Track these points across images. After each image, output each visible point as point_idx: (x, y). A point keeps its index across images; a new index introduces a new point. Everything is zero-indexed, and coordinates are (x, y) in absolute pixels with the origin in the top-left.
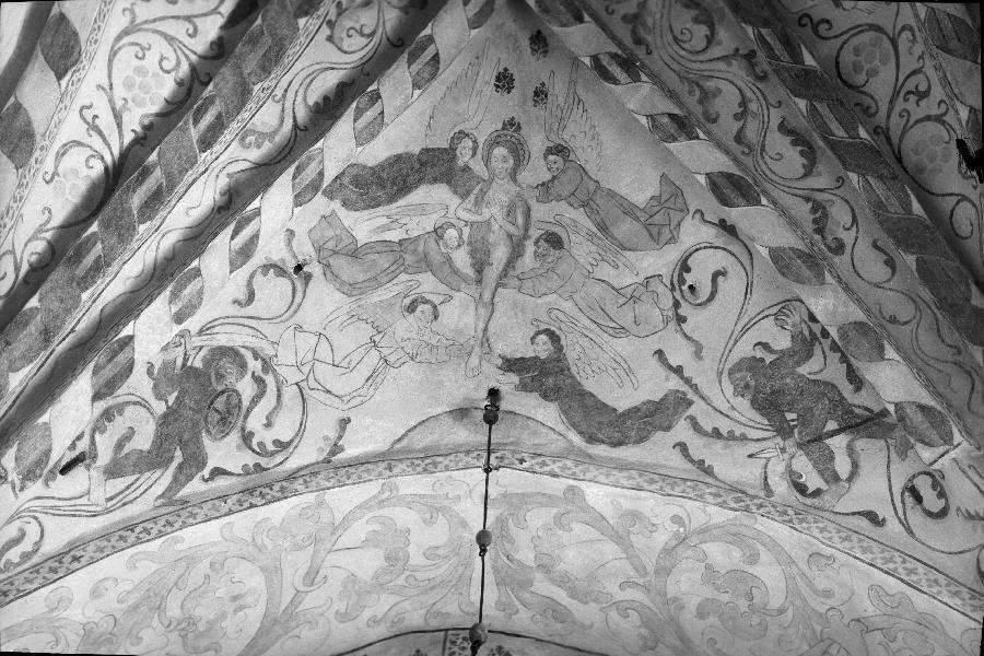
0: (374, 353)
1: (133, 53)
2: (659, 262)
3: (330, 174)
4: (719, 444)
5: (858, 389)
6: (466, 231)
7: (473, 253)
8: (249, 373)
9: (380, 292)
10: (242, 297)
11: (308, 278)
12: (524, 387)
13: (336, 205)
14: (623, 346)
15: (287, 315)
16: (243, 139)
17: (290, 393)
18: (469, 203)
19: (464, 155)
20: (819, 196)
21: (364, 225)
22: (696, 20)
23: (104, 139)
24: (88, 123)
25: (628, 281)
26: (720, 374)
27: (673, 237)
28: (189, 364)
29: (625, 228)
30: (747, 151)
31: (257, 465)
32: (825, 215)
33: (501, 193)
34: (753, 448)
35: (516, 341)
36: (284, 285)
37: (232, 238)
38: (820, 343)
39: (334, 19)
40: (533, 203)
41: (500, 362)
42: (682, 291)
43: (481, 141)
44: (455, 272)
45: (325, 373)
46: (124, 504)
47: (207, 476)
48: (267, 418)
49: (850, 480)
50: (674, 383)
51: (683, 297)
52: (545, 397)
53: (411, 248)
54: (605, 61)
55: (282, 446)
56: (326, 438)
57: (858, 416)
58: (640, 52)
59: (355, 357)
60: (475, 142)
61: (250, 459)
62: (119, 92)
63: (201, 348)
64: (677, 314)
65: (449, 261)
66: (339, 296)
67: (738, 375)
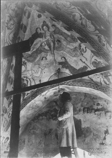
0: (40, 69)
7: (48, 45)
9: (37, 59)
12: (63, 67)
17: (31, 80)
19: (39, 31)
26: (91, 64)
29: (69, 39)
32: (100, 39)
33: (48, 34)
34: (98, 76)
35: (59, 59)
40: (53, 34)
41: (58, 63)
43: (41, 27)
44: (46, 50)
45: (35, 75)
50: (84, 65)
52: (66, 68)
53: (38, 50)
60: (40, 28)
65: (45, 49)
66: (31, 63)
67: (93, 64)
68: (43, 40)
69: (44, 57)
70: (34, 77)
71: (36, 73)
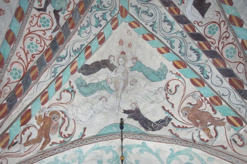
0: (92, 111)
1: (30, 39)
2: (163, 84)
3: (79, 67)
4: (180, 130)
6: (113, 79)
8: (61, 118)
10: (59, 98)
11: (75, 92)
12: (129, 117)
13: (81, 74)
14: (153, 106)
15: (71, 101)
16: (58, 59)
20: (202, 65)
21: (88, 79)
22: (168, 24)
23: (23, 60)
24: (19, 57)
25: (154, 89)
26: (179, 111)
28: (46, 116)
30: (182, 55)
31: (63, 141)
32: (203, 70)
34: (189, 130)
36: (69, 95)
37: (56, 83)
38: (204, 102)
39: (79, 30)
40: (129, 71)
41: (123, 111)
42: (168, 91)
44: (111, 90)
47: (51, 144)
48: (66, 128)
49: (216, 137)
50: (167, 115)
51: (168, 92)
54: (146, 35)
55: (70, 135)
56: (81, 133)
57: (216, 120)
58: (154, 33)
61: (62, 139)
62: (26, 49)
63: (49, 111)
64: (167, 97)
65: (109, 87)
66: (83, 97)
67: (184, 111)
68: (112, 74)
69: (104, 97)
70: (78, 119)
71: (84, 115)
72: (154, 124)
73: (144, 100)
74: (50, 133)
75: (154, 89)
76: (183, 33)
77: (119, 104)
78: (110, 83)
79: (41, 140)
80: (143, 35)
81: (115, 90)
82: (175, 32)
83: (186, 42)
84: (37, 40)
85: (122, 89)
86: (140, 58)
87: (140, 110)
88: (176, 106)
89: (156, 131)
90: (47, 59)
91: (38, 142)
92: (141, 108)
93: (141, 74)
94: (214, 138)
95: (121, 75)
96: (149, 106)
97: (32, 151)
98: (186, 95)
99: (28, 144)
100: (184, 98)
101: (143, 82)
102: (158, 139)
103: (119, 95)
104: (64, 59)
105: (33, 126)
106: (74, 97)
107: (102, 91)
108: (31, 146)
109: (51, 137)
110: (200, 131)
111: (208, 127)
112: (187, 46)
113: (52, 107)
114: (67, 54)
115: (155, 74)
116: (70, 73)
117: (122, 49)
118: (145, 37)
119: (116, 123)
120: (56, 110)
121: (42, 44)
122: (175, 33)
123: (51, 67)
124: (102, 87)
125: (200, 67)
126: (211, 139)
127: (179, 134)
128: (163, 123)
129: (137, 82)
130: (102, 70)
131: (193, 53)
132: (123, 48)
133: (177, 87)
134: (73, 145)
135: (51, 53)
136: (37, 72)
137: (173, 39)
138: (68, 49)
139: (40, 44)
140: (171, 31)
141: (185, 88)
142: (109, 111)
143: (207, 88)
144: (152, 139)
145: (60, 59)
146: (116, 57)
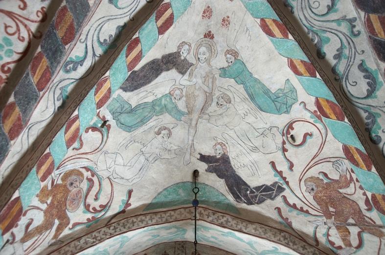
2: (281, 120)
4: (295, 212)
5: (369, 210)
6: (184, 90)
8: (85, 181)
11: (109, 127)
14: (255, 156)
15: (102, 146)
18: (186, 76)
20: (373, 110)
21: (134, 98)
26: (300, 180)
27: (287, 111)
28: (55, 183)
34: (312, 218)
36: (97, 135)
37: (65, 133)
38: (355, 183)
40: (217, 76)
41: (199, 156)
42: (287, 137)
44: (179, 111)
46: (35, 249)
47: (71, 227)
48: (96, 196)
50: (277, 179)
51: (288, 140)
54: (269, 22)
55: (104, 207)
57: (367, 222)
59: (134, 161)
61: (90, 216)
63: (60, 174)
64: (283, 147)
65: (176, 107)
67: (309, 183)
68: (184, 80)
69: (165, 129)
71: (128, 167)
72: (252, 192)
73: (240, 142)
74: (66, 211)
75: (261, 125)
76: (354, 24)
77: (193, 141)
78: (178, 97)
79: (52, 225)
80: (263, 20)
81: (186, 110)
82: (336, 18)
83: (355, 48)
84: (6, 27)
85: (200, 112)
86: (244, 55)
87: (230, 158)
88: (298, 169)
89: (253, 206)
90: (38, 82)
91: (47, 229)
92: (232, 156)
93: (241, 88)
94: (353, 248)
95: (200, 81)
96: (248, 155)
97: (37, 245)
98: (320, 157)
99: (30, 237)
100: (316, 160)
101: (242, 106)
102: (256, 229)
103: (194, 123)
104: (81, 65)
105: (33, 209)
106: (108, 137)
107: (161, 117)
108: (35, 238)
109: (69, 216)
110: (330, 228)
111: (348, 227)
112: (352, 59)
113: (65, 164)
114: (86, 52)
115: (270, 97)
116: (94, 106)
117: (208, 26)
118: (267, 26)
119: (185, 181)
120: (74, 168)
121: (21, 35)
122: (337, 21)
123: (54, 88)
124: (161, 109)
125: (370, 113)
126: (348, 248)
127: (292, 221)
128: (268, 192)
129: (230, 102)
130: (164, 74)
131: (362, 78)
132: (209, 24)
133: (308, 136)
134: (109, 228)
135: (45, 67)
136: (19, 119)
137: (328, 35)
138: (88, 39)
139: (16, 35)
140: (327, 13)
141: (323, 144)
142: (175, 156)
143: (376, 176)
144: (246, 229)
145: (71, 66)
146: (193, 46)
